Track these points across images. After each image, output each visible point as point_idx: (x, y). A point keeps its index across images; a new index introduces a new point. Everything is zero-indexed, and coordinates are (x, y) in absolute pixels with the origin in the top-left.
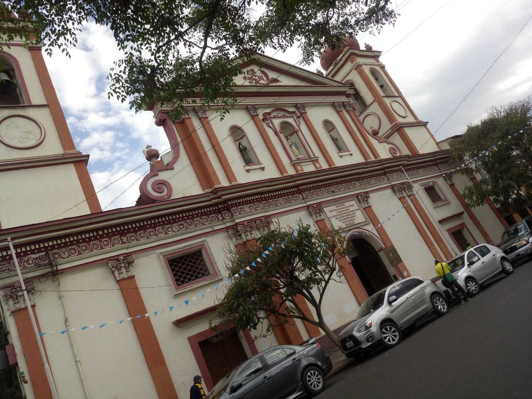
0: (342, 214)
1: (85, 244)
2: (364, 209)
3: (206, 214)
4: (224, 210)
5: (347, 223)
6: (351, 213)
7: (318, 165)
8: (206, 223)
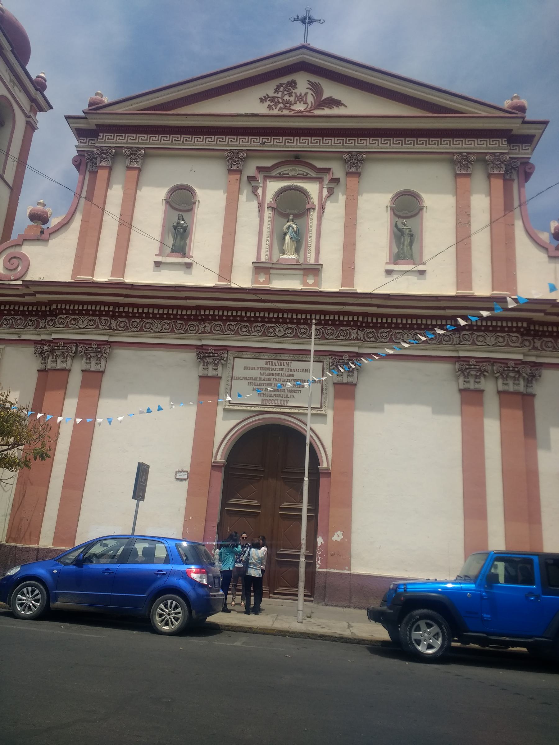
2: (334, 384)
3: (23, 313)
4: (50, 316)
5: (268, 398)
8: (16, 327)
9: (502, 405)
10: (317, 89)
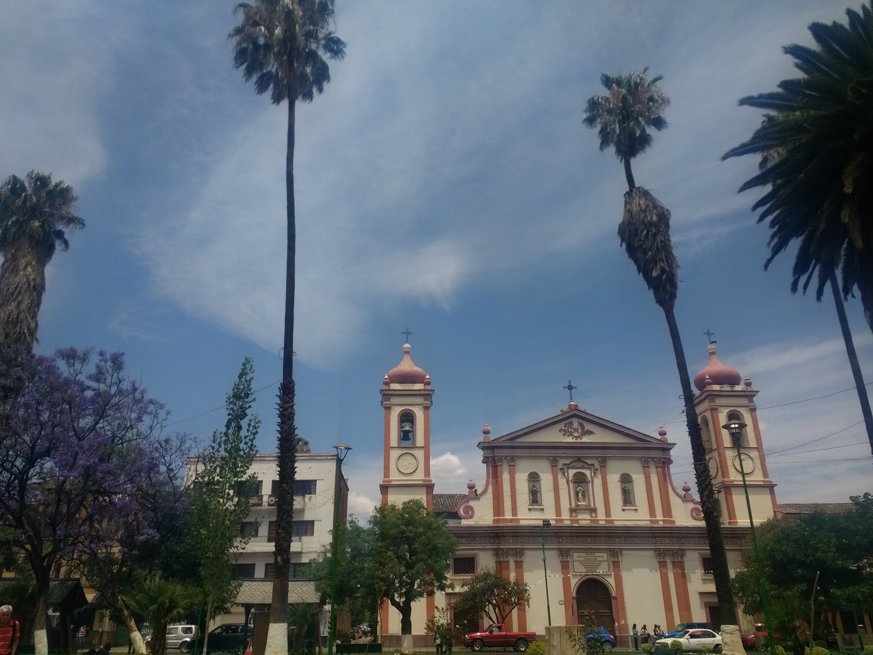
0: (588, 561)
7: (594, 515)
9: (674, 567)
10: (583, 427)
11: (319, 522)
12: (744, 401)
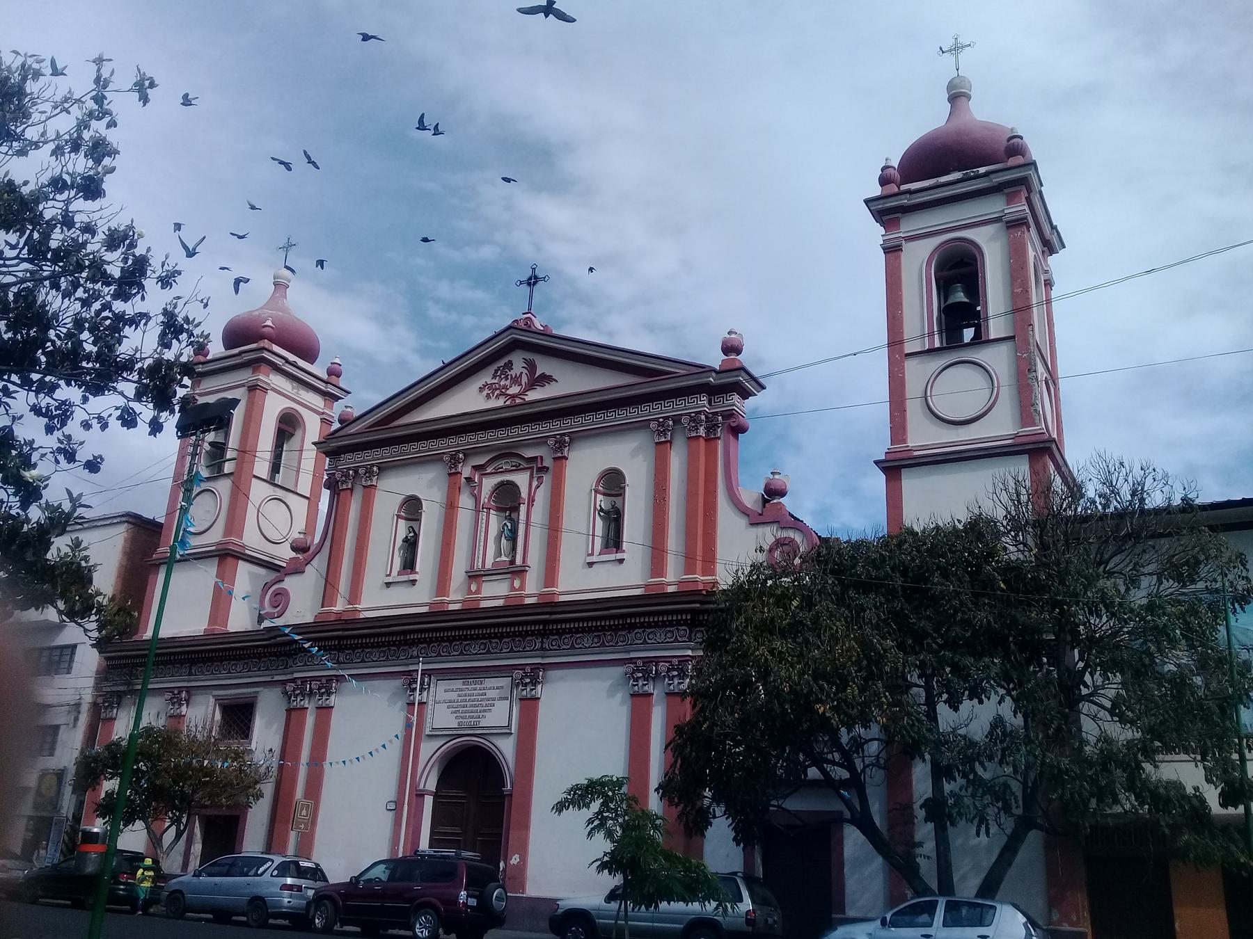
1: (162, 667)
2: (520, 699)
3: (275, 655)
6: (484, 703)
10: (531, 367)
11: (83, 645)
12: (994, 206)
